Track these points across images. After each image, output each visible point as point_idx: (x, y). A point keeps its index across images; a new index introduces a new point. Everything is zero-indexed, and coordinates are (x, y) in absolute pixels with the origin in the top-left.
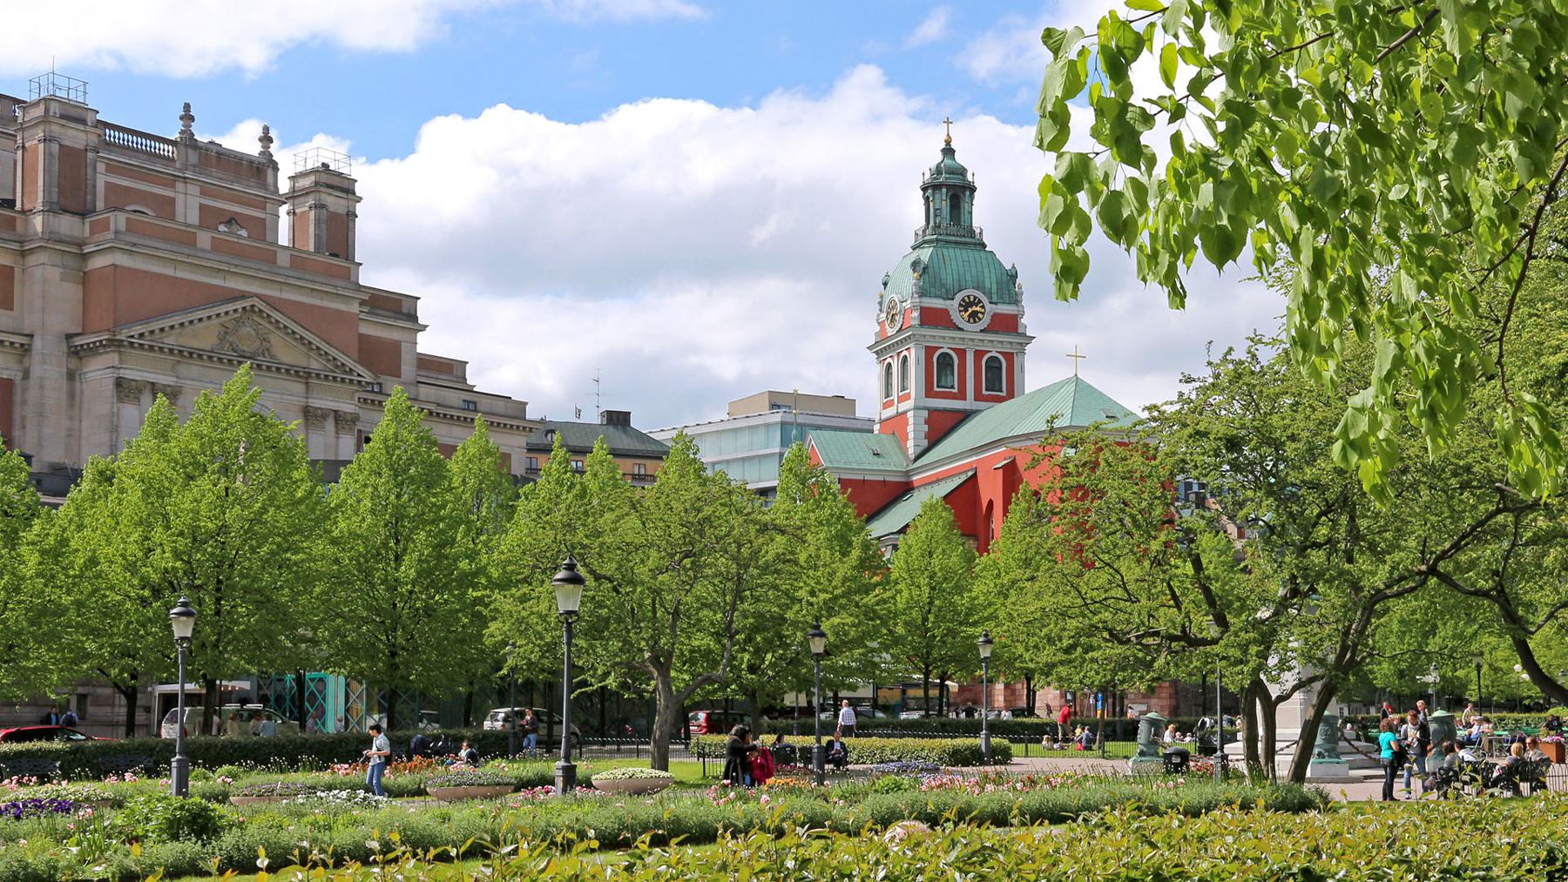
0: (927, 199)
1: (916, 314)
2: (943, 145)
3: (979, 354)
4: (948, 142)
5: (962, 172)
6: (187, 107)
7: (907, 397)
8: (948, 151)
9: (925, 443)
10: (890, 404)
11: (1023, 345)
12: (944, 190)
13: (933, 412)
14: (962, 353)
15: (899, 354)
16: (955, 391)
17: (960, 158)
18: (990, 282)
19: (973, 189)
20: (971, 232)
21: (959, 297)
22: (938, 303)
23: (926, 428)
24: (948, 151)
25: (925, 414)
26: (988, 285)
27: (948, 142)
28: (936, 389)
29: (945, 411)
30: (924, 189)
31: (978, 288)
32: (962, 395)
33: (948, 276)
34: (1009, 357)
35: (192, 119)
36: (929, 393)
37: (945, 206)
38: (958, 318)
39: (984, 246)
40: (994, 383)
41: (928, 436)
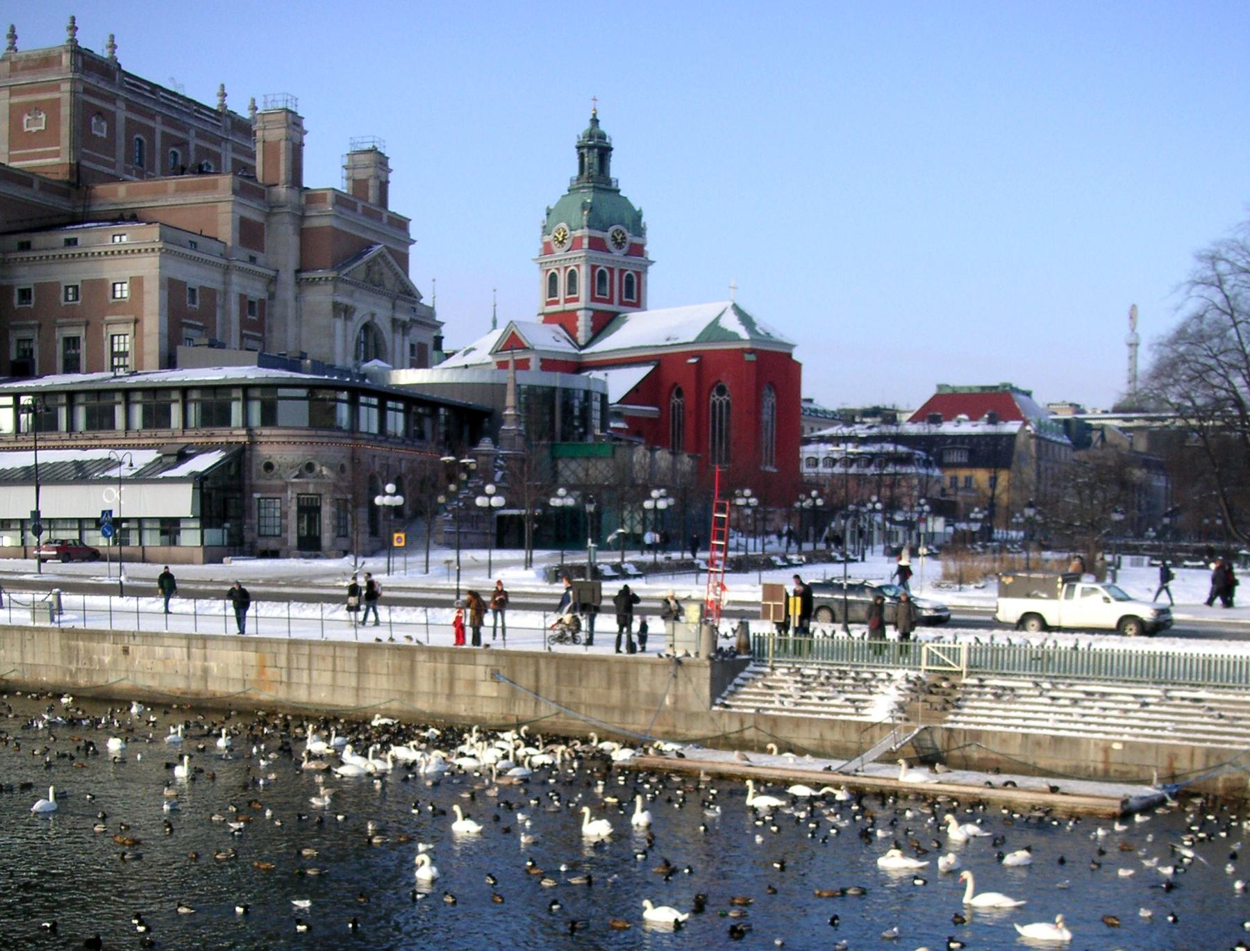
0: (582, 157)
1: (586, 241)
2: (591, 117)
3: (622, 271)
4: (594, 115)
5: (602, 136)
6: (13, 29)
7: (577, 300)
8: (595, 121)
9: (590, 335)
10: (557, 302)
11: (646, 266)
12: (596, 150)
13: (596, 312)
14: (611, 270)
15: (566, 268)
16: (608, 298)
17: (603, 127)
18: (628, 221)
19: (611, 149)
20: (609, 182)
21: (612, 229)
22: (598, 234)
23: (591, 324)
24: (595, 121)
25: (591, 313)
26: (627, 222)
27: (594, 115)
28: (597, 296)
29: (603, 312)
30: (579, 148)
31: (620, 224)
32: (610, 301)
33: (604, 215)
34: (638, 274)
35: (16, 37)
36: (593, 299)
37: (596, 161)
38: (610, 244)
39: (618, 191)
40: (629, 295)
41: (593, 329)
